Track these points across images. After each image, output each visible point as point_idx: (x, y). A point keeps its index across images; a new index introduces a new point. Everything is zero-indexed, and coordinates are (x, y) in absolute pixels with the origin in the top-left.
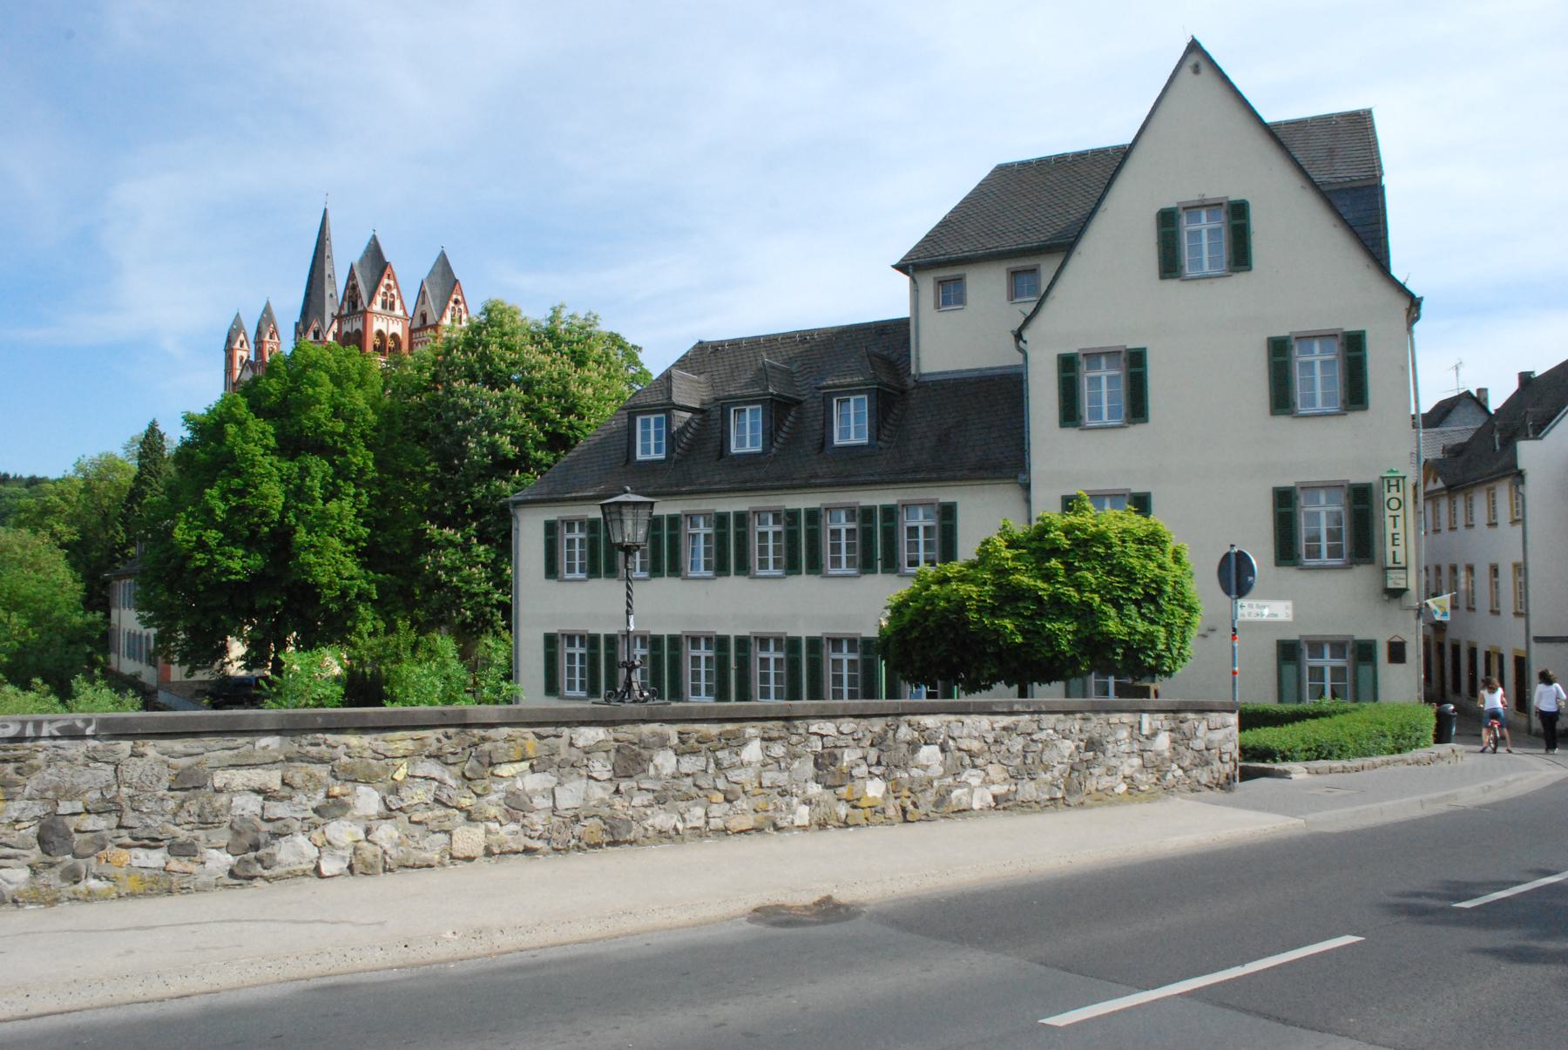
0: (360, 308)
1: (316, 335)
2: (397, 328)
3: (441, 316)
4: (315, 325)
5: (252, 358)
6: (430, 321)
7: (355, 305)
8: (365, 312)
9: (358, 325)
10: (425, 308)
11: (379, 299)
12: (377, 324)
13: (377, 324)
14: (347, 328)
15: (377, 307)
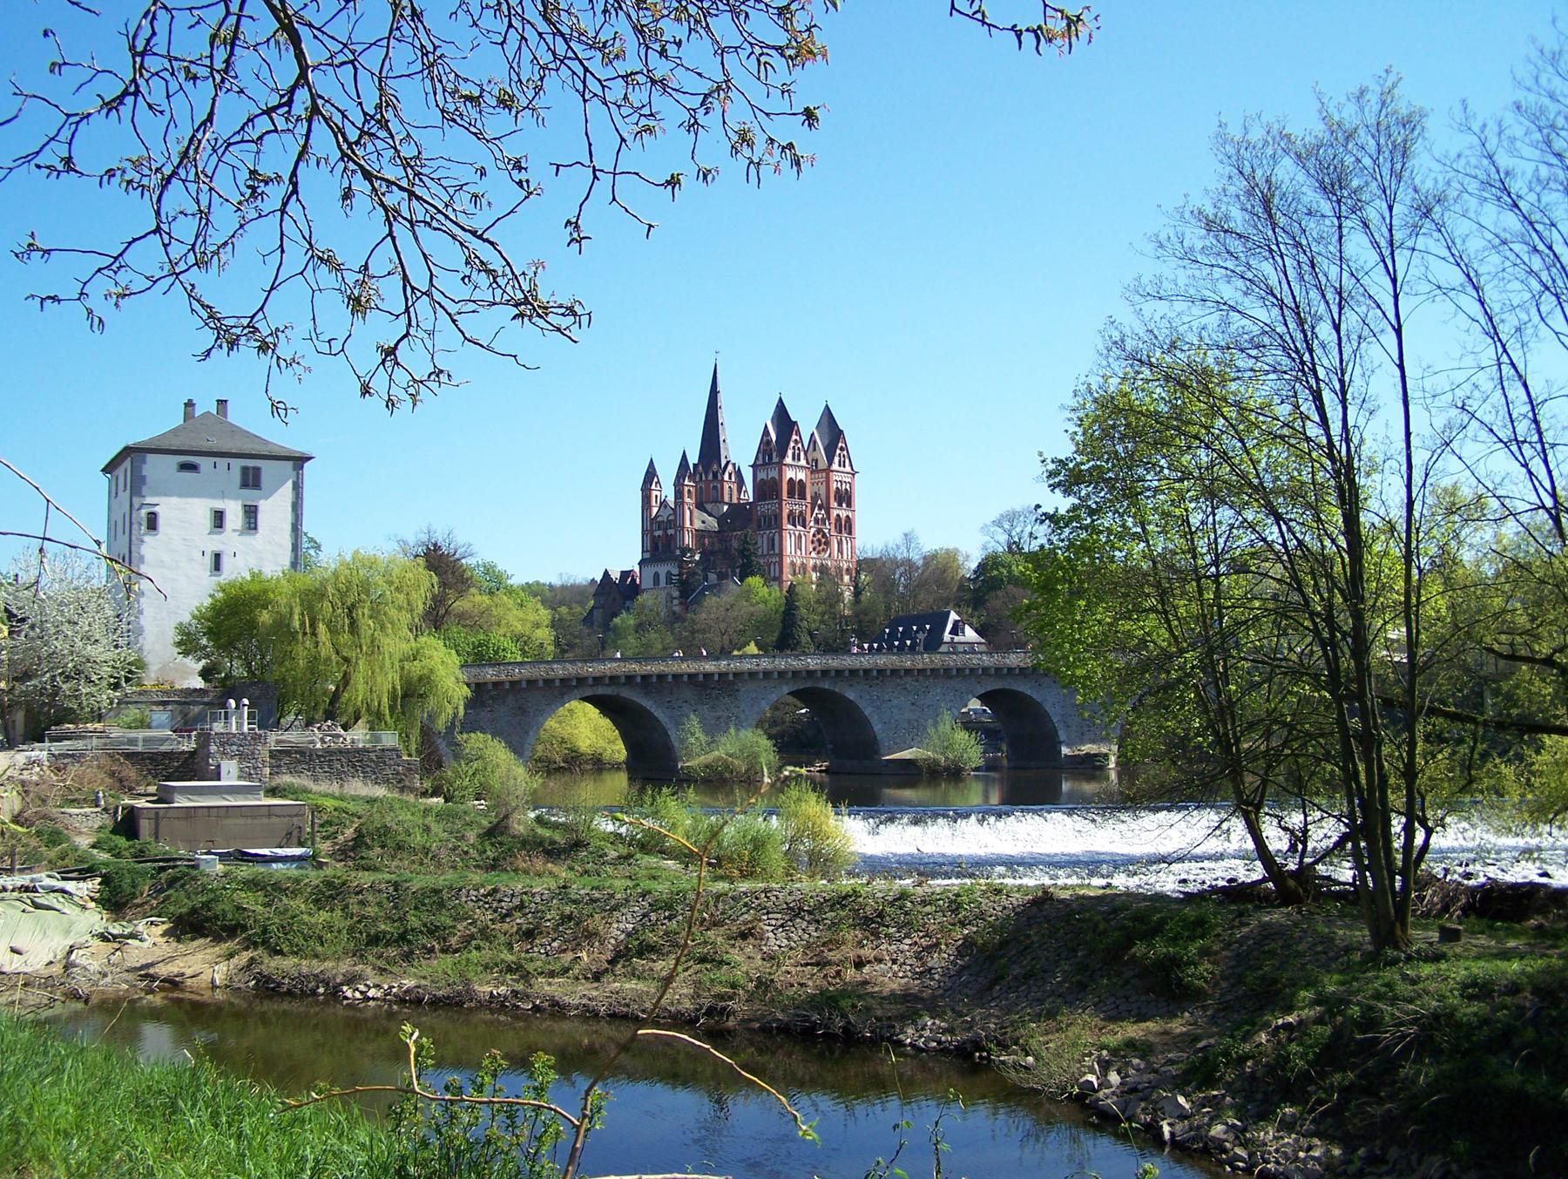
0: (775, 459)
1: (715, 476)
2: (801, 475)
3: (830, 462)
4: (715, 467)
5: (671, 499)
6: (821, 466)
7: (770, 458)
8: (781, 464)
9: (774, 474)
10: (816, 455)
11: (790, 453)
12: (789, 474)
13: (789, 474)
14: (762, 475)
15: (788, 460)
